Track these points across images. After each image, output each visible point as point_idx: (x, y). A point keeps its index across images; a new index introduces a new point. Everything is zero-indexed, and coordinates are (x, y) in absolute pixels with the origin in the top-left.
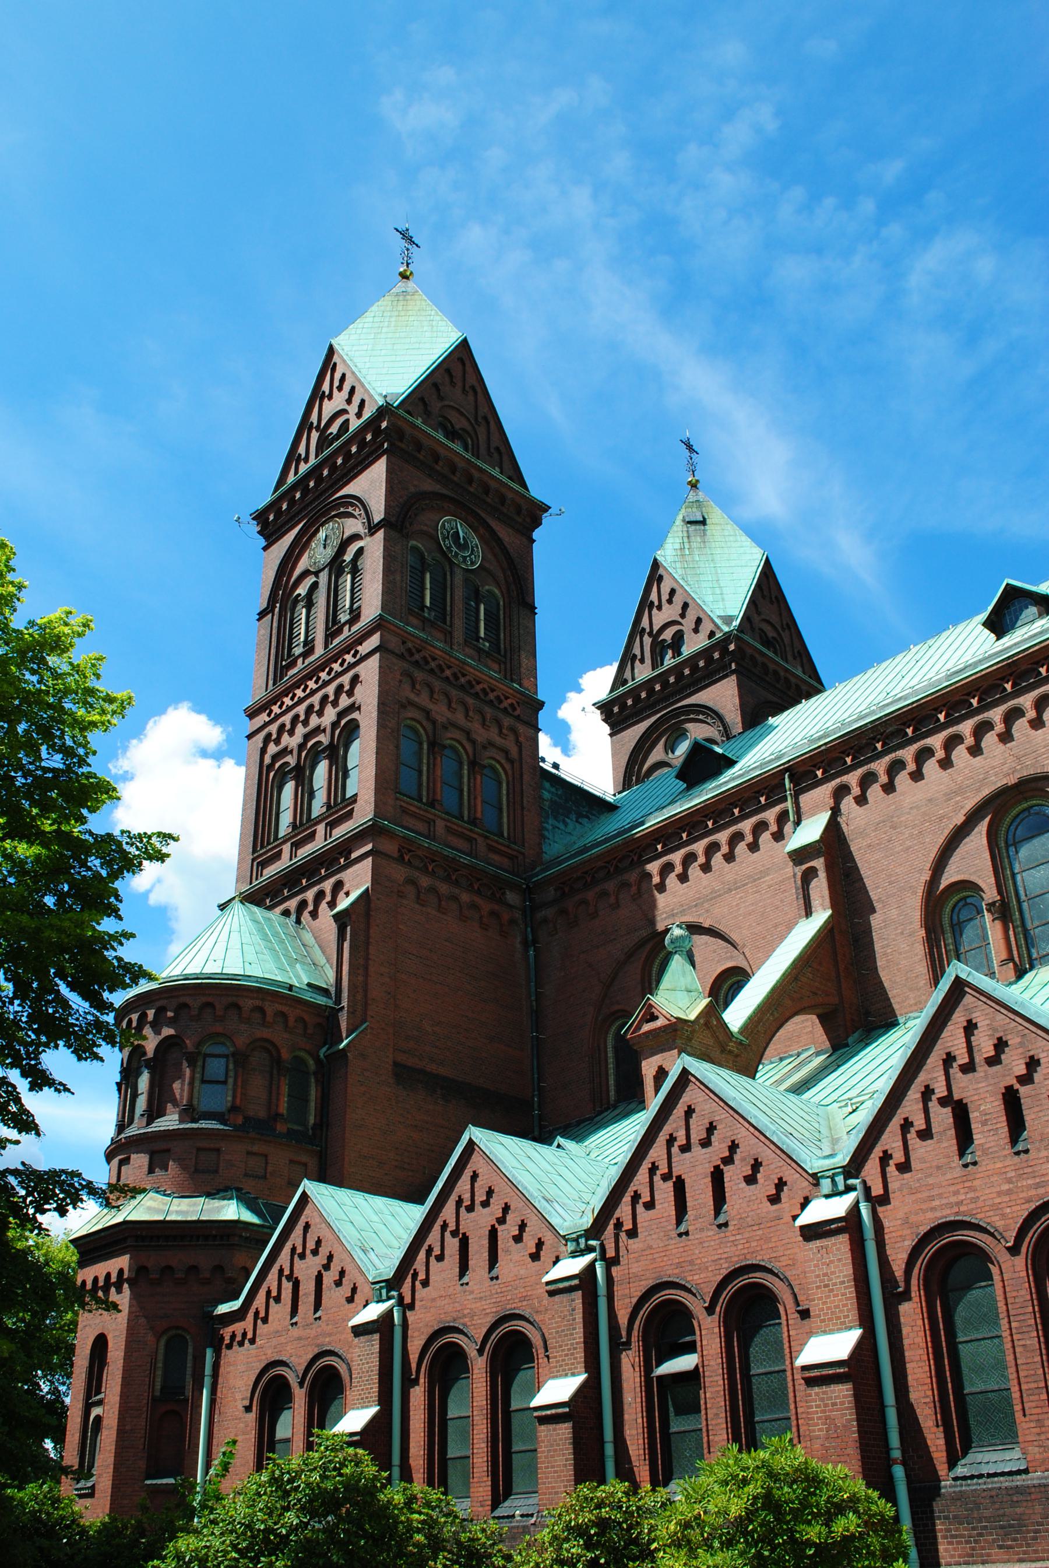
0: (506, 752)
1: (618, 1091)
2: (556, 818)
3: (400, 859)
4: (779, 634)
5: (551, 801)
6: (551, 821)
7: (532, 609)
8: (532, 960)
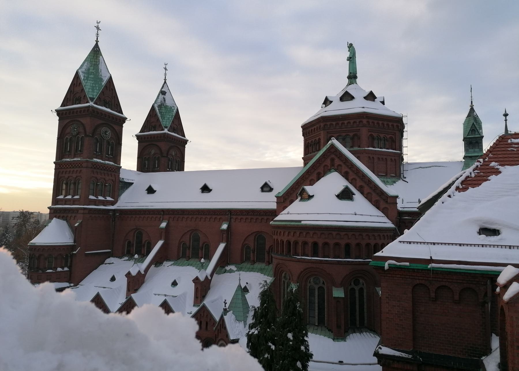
0: (112, 180)
1: (127, 252)
2: (122, 190)
3: (89, 213)
4: (178, 127)
5: (122, 186)
6: (121, 191)
7: (121, 145)
8: (114, 224)
